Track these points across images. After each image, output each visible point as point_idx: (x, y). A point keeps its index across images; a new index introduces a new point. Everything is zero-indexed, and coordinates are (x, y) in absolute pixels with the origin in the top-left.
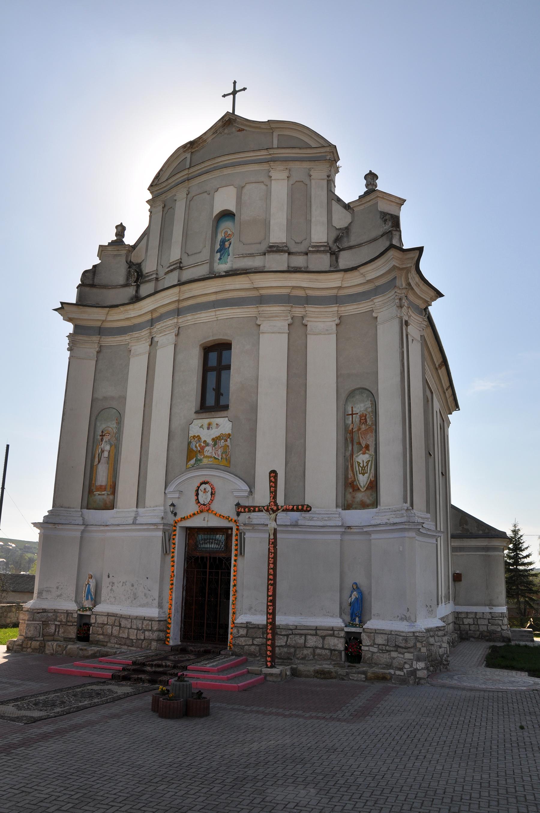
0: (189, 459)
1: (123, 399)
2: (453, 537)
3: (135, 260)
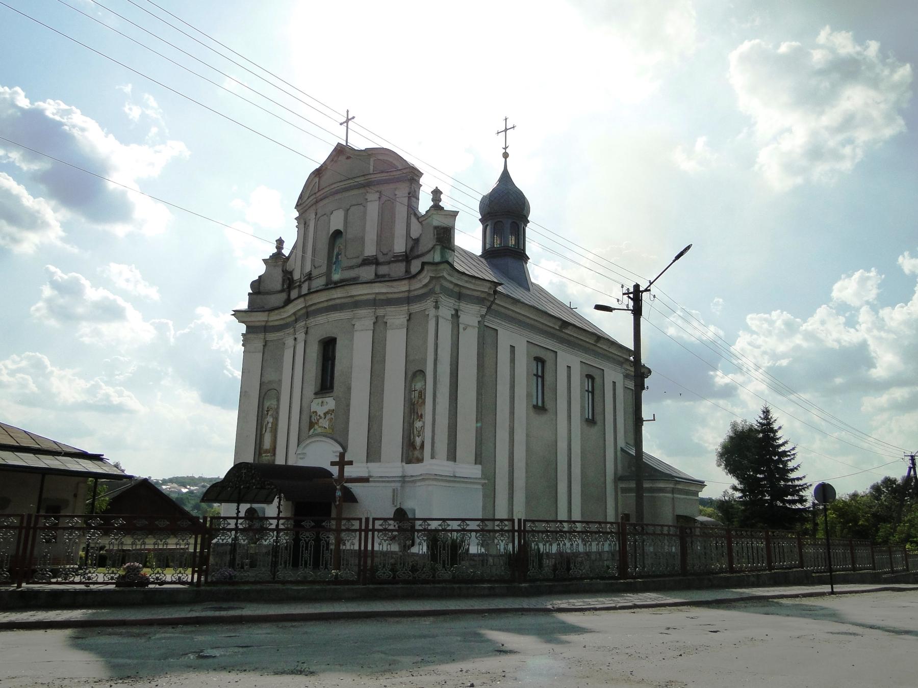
0: (310, 430)
1: (280, 381)
2: (618, 479)
3: (289, 268)
